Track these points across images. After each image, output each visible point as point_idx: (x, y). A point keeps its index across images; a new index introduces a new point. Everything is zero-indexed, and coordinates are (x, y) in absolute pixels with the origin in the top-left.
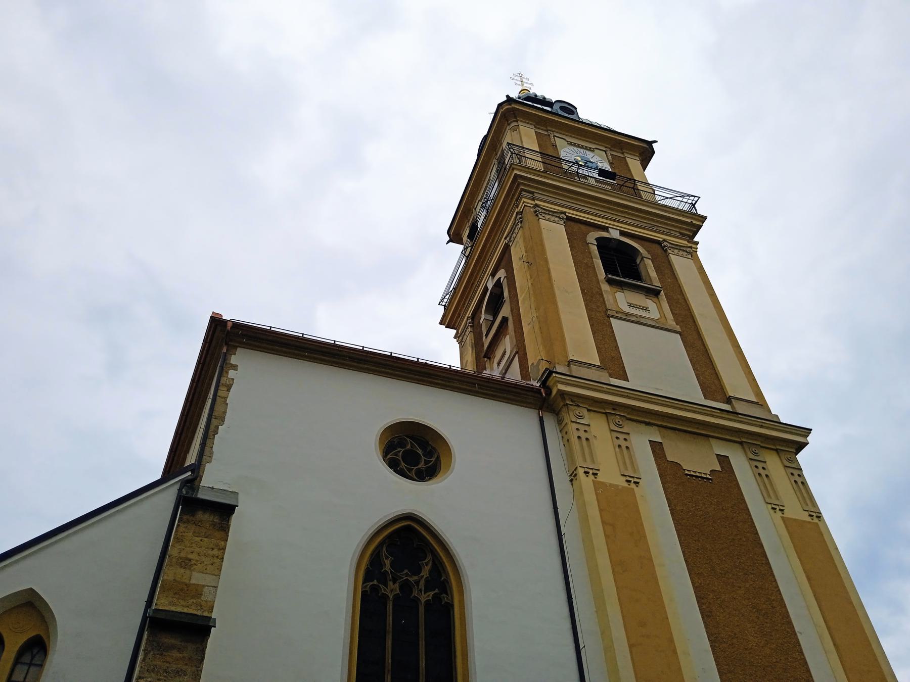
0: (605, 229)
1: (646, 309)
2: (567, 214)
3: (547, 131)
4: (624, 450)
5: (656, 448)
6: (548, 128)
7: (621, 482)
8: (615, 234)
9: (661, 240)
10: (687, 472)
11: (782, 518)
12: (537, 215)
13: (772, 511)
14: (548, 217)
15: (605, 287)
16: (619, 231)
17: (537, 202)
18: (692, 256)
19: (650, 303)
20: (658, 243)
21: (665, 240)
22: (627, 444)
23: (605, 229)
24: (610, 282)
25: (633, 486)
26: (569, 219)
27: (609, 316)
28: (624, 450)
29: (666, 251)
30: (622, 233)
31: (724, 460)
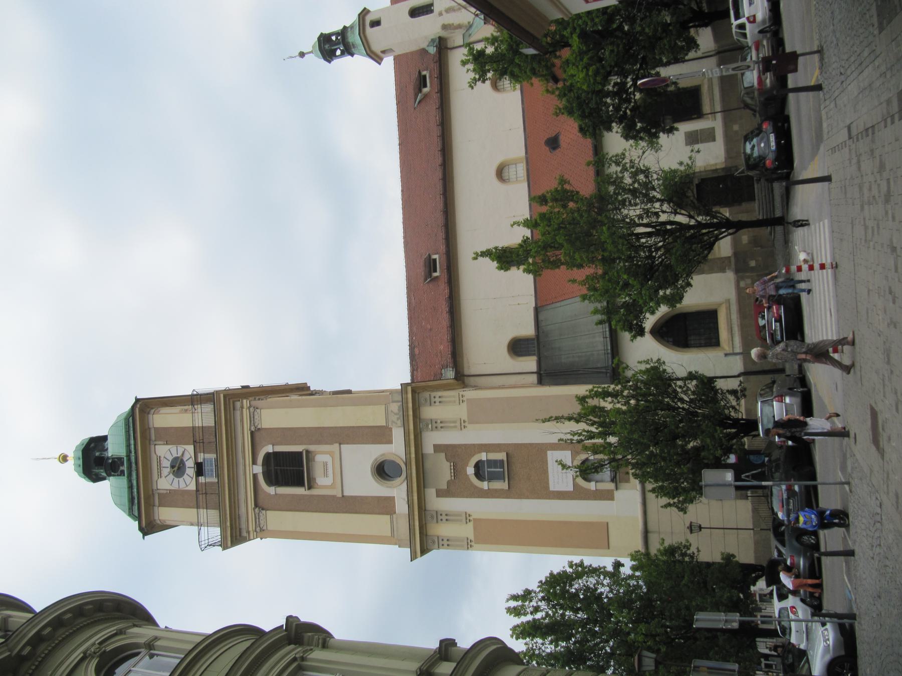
0: (255, 476)
1: (325, 465)
2: (253, 506)
3: (153, 494)
4: (449, 517)
5: (440, 494)
6: (151, 493)
7: (471, 525)
8: (258, 469)
9: (249, 432)
10: (453, 478)
11: (469, 423)
12: (263, 530)
13: (466, 429)
14: (262, 522)
15: (314, 492)
16: (254, 466)
17: (251, 529)
18: (257, 408)
19: (320, 458)
20: (252, 433)
21: (250, 429)
22: (444, 515)
23: (255, 476)
24: (310, 488)
25: (471, 518)
26: (256, 505)
27: (343, 496)
28: (449, 517)
29: (259, 429)
30: (254, 462)
31: (438, 448)
